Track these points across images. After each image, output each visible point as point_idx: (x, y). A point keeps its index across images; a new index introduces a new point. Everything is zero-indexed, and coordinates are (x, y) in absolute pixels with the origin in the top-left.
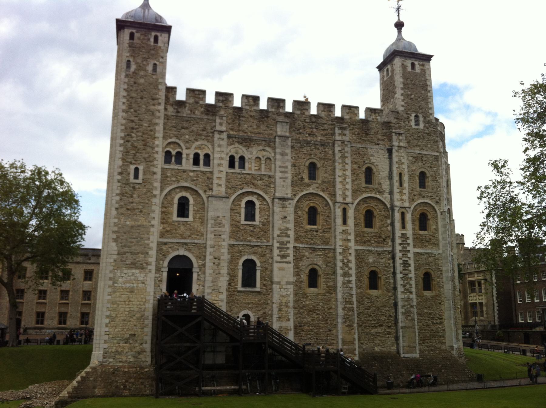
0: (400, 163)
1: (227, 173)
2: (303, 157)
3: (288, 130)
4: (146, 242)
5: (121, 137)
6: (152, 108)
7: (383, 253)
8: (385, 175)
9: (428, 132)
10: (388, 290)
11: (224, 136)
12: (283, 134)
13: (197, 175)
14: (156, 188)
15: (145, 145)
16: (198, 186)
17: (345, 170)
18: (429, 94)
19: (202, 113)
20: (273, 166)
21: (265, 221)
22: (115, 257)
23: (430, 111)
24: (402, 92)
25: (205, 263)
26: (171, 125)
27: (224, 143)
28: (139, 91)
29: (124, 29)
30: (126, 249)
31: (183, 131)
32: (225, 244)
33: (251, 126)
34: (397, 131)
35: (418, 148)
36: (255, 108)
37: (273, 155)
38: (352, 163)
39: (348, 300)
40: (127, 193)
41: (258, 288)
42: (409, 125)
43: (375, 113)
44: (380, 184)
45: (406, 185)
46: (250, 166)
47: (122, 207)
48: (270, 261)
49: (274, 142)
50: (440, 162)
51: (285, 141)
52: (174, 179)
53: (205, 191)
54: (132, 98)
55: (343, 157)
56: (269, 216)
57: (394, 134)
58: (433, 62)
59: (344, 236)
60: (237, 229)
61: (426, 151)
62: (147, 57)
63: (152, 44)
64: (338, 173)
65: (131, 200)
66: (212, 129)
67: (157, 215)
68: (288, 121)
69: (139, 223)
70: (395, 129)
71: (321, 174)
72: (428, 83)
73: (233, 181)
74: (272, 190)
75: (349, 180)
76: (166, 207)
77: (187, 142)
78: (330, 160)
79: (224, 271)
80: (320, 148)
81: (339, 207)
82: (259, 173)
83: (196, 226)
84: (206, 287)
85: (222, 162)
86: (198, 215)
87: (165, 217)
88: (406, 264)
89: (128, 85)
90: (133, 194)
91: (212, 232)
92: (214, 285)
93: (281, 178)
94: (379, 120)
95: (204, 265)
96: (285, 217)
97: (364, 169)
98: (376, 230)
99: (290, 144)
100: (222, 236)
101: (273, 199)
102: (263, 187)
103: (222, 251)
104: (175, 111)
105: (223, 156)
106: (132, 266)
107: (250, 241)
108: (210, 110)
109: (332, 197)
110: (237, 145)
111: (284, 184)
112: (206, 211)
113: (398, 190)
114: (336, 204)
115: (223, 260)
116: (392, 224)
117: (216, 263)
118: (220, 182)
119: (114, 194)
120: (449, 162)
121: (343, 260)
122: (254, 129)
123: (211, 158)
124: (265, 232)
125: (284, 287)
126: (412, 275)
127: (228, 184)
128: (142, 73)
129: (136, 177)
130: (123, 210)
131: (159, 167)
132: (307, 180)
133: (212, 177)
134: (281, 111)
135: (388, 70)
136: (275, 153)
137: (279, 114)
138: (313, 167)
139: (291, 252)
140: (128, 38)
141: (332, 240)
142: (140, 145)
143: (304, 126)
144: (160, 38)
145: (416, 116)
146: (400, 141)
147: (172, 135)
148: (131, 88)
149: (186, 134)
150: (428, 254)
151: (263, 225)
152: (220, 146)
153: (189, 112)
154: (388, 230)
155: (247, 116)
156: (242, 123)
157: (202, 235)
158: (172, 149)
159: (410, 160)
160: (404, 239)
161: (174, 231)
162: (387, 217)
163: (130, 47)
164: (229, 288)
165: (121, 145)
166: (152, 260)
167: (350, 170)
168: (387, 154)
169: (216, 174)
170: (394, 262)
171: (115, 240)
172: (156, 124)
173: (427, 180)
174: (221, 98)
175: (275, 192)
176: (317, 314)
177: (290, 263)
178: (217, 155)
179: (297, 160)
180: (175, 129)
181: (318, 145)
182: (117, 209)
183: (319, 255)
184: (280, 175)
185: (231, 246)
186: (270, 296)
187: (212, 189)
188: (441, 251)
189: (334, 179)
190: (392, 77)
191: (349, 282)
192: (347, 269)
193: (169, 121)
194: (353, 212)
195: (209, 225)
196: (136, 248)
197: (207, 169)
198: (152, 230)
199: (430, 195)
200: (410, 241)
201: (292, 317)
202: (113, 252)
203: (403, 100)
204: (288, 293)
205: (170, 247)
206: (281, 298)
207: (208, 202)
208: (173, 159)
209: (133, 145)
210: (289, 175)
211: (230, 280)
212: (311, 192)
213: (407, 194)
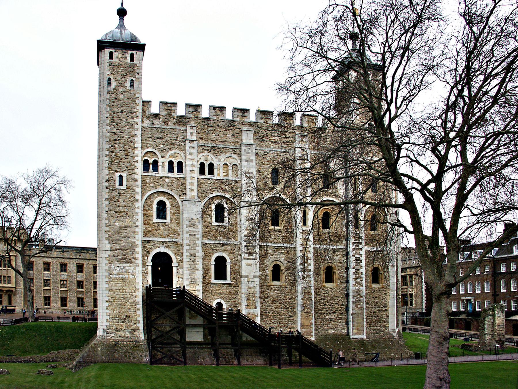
3: (252, 138)
4: (132, 240)
10: (342, 283)
14: (138, 193)
16: (173, 191)
19: (174, 124)
22: (109, 253)
25: (182, 259)
26: (147, 136)
27: (194, 151)
28: (120, 105)
30: (117, 247)
31: (158, 141)
32: (199, 242)
37: (239, 161)
39: (306, 291)
40: (114, 198)
41: (228, 281)
46: (218, 172)
48: (239, 257)
52: (152, 185)
53: (180, 196)
54: (114, 112)
63: (129, 61)
67: (140, 217)
69: (126, 224)
76: (147, 210)
79: (200, 266)
83: (173, 227)
84: (185, 280)
85: (194, 169)
86: (174, 217)
88: (358, 261)
91: (187, 232)
92: (191, 278)
95: (182, 261)
100: (196, 236)
103: (197, 248)
104: (151, 123)
105: (195, 163)
107: (220, 240)
108: (182, 120)
110: (206, 153)
115: (198, 256)
123: (184, 165)
124: (234, 232)
125: (251, 280)
126: (363, 270)
128: (121, 89)
129: (121, 184)
130: (112, 213)
136: (241, 160)
137: (243, 123)
139: (257, 250)
140: (108, 58)
144: (135, 56)
148: (113, 104)
152: (191, 154)
153: (163, 124)
155: (215, 125)
156: (210, 132)
157: (179, 235)
164: (204, 281)
166: (139, 256)
169: (188, 181)
171: (108, 239)
174: (191, 109)
176: (280, 303)
178: (189, 163)
185: (205, 244)
186: (239, 288)
187: (185, 194)
191: (308, 276)
195: (185, 226)
196: (124, 246)
198: (137, 230)
201: (258, 305)
202: (107, 249)
204: (255, 285)
206: (249, 290)
208: (151, 166)
209: (116, 155)
211: (204, 273)
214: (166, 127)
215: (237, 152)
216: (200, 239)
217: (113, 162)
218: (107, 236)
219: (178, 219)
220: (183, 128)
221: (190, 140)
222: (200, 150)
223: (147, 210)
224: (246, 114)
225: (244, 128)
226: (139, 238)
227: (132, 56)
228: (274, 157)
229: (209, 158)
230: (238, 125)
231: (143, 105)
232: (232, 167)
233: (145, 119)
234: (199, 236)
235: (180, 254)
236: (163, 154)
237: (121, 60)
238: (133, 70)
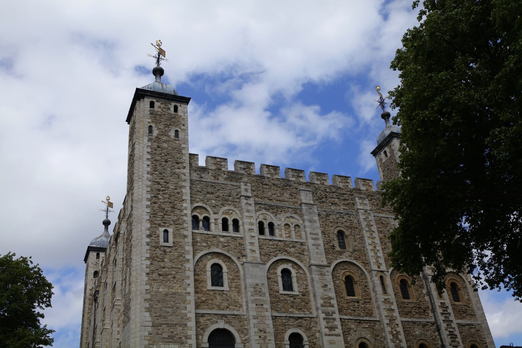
1: (259, 239)
2: (330, 225)
3: (312, 199)
4: (182, 312)
5: (147, 199)
7: (427, 325)
11: (251, 201)
12: (308, 202)
13: (227, 240)
14: (188, 251)
16: (230, 252)
17: (374, 238)
21: (304, 290)
22: (150, 329)
27: (252, 208)
32: (268, 314)
33: (275, 194)
36: (276, 177)
37: (301, 222)
40: (157, 257)
47: (153, 272)
49: (301, 210)
52: (205, 244)
54: (156, 160)
55: (369, 226)
59: (388, 306)
60: (277, 299)
62: (169, 124)
63: (173, 112)
64: (368, 241)
65: (162, 264)
66: (237, 195)
69: (173, 291)
71: (350, 243)
73: (265, 248)
74: (306, 258)
75: (379, 248)
76: (198, 275)
77: (213, 207)
78: (357, 228)
80: (344, 217)
81: (376, 276)
83: (233, 296)
85: (253, 227)
86: (234, 284)
91: (253, 302)
93: (314, 245)
98: (415, 301)
99: (316, 211)
100: (265, 306)
103: (267, 322)
104: (199, 176)
105: (253, 221)
106: (170, 340)
107: (292, 313)
110: (264, 211)
115: (269, 333)
116: (429, 294)
117: (262, 337)
118: (254, 248)
119: (144, 258)
121: (392, 332)
122: (278, 196)
123: (240, 223)
124: (307, 303)
128: (164, 138)
129: (166, 240)
130: (155, 276)
132: (338, 248)
134: (301, 180)
135: (385, 153)
136: (304, 220)
138: (340, 234)
139: (338, 323)
140: (149, 106)
141: (376, 312)
142: (168, 207)
144: (179, 108)
147: (198, 199)
148: (155, 152)
149: (212, 199)
150: (469, 325)
151: (303, 295)
152: (248, 211)
153: (213, 178)
154: (425, 301)
155: (270, 184)
156: (265, 190)
157: (241, 306)
158: (199, 213)
160: (444, 309)
161: (210, 301)
165: (147, 207)
166: (192, 333)
169: (248, 240)
170: (440, 334)
171: (148, 310)
172: (184, 187)
174: (242, 166)
175: (310, 260)
177: (340, 335)
178: (246, 220)
179: (325, 228)
180: (200, 194)
181: (342, 213)
182: (147, 274)
183: (366, 328)
185: (274, 318)
188: (479, 322)
192: (397, 342)
195: (249, 294)
198: (188, 298)
200: (450, 310)
202: (147, 324)
205: (208, 320)
208: (201, 223)
209: (159, 207)
210: (321, 242)
212: (345, 260)
214: (216, 181)
216: (269, 310)
217: (156, 214)
218: (148, 306)
219: (238, 287)
221: (245, 196)
223: (198, 275)
224: (301, 175)
226: (191, 311)
227: (176, 109)
228: (337, 219)
229: (268, 217)
230: (294, 185)
231: (190, 158)
233: (192, 171)
234: (267, 306)
235: (244, 331)
237: (164, 110)
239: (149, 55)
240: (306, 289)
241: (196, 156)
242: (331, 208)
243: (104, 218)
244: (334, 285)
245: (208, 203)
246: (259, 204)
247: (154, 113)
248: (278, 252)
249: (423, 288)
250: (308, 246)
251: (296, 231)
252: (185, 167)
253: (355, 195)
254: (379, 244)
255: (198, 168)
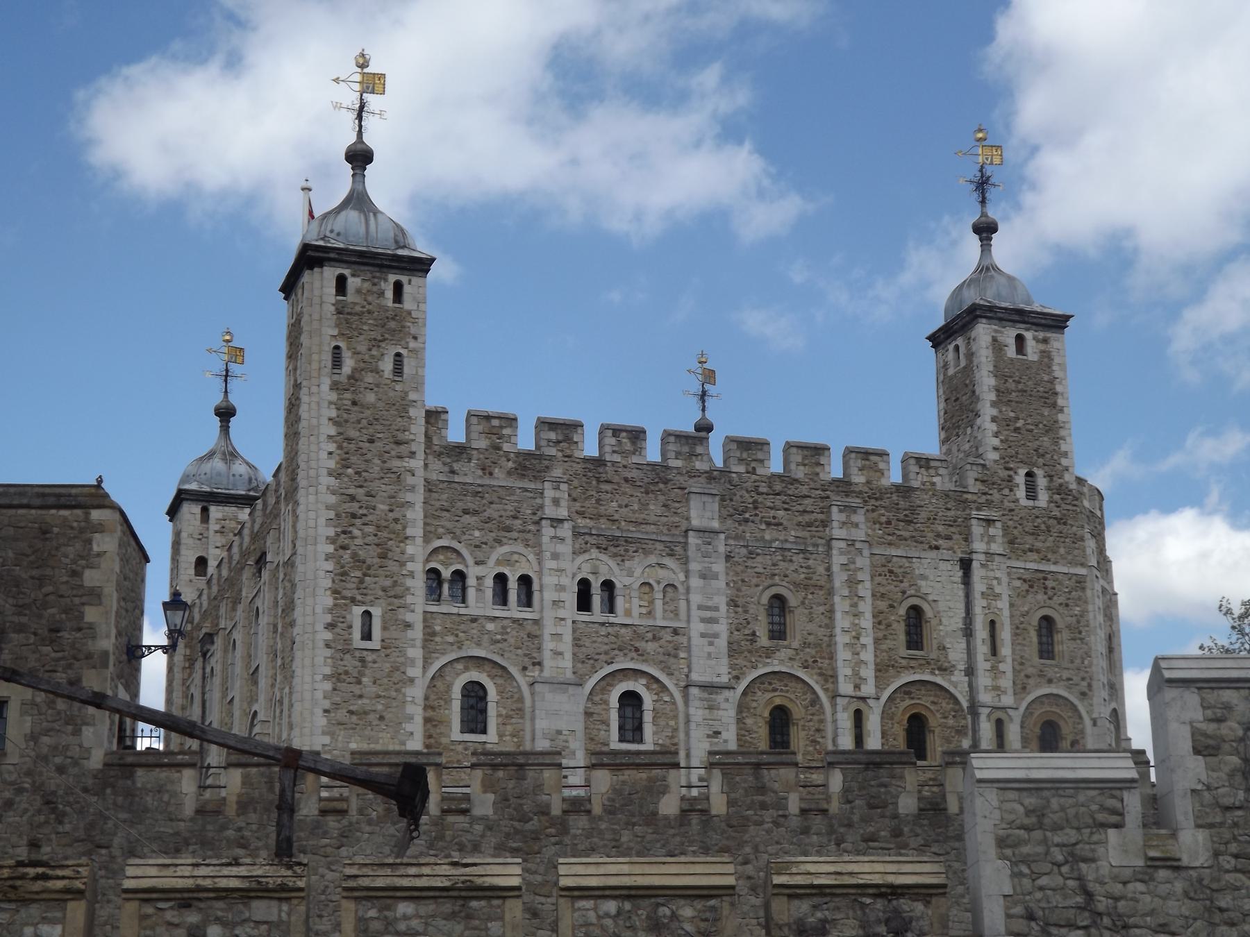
0: (990, 595)
3: (716, 516)
5: (327, 538)
6: (396, 463)
8: (954, 627)
9: (1058, 514)
11: (566, 531)
13: (504, 628)
15: (383, 556)
18: (1061, 417)
20: (683, 604)
23: (1064, 462)
24: (994, 412)
26: (438, 504)
27: (566, 549)
28: (364, 422)
29: (321, 266)
31: (467, 519)
34: (984, 514)
35: (1034, 556)
36: (635, 459)
37: (682, 577)
38: (873, 595)
40: (346, 673)
42: (1011, 498)
43: (928, 468)
44: (944, 648)
45: (1006, 651)
46: (627, 605)
49: (685, 545)
50: (1089, 593)
51: (709, 544)
52: (451, 639)
53: (525, 669)
54: (349, 440)
55: (853, 583)
56: (675, 730)
57: (974, 522)
58: (1068, 343)
61: (1055, 563)
62: (380, 338)
63: (390, 304)
64: (842, 622)
65: (357, 690)
66: (534, 514)
68: (714, 492)
70: (978, 509)
71: (799, 624)
72: (1059, 388)
75: (867, 640)
76: (433, 708)
77: (476, 546)
81: (845, 709)
82: (651, 623)
85: (564, 596)
86: (509, 727)
87: (432, 731)
89: (338, 409)
90: (362, 674)
93: (703, 635)
94: (939, 487)
96: (717, 733)
97: (902, 611)
101: (687, 687)
102: (661, 658)
104: (447, 469)
105: (565, 581)
108: (529, 465)
109: (826, 681)
110: (594, 553)
111: (711, 649)
112: (528, 716)
113: (988, 665)
114: (839, 700)
118: (561, 647)
120: (1117, 587)
122: (634, 512)
123: (535, 586)
127: (577, 649)
128: (369, 378)
129: (367, 636)
130: (341, 714)
131: (419, 609)
132: (764, 641)
133: (538, 633)
134: (699, 465)
135: (957, 348)
136: (687, 574)
138: (779, 603)
142: (370, 555)
143: (755, 502)
144: (407, 289)
145: (1029, 474)
146: (991, 539)
147: (441, 530)
148: (345, 416)
152: (555, 556)
153: (480, 472)
155: (616, 479)
158: (443, 563)
159: (1015, 588)
162: (961, 732)
163: (339, 312)
165: (328, 557)
167: (868, 615)
168: (960, 574)
169: (549, 628)
172: (409, 504)
173: (1057, 637)
175: (690, 671)
178: (550, 580)
179: (739, 590)
182: (326, 711)
184: (702, 627)
187: (539, 664)
189: (832, 636)
190: (969, 370)
193: (434, 495)
194: (879, 719)
197: (527, 614)
199: (1065, 675)
203: (996, 435)
207: (532, 694)
208: (446, 586)
209: (354, 556)
210: (722, 628)
212: (776, 669)
213: (1010, 675)
214: (487, 481)
215: (676, 549)
220: (532, 486)
221: (551, 519)
222: (577, 546)
223: (433, 708)
224: (699, 450)
225: (695, 485)
227: (398, 287)
230: (678, 477)
231: (427, 422)
232: (664, 592)
233: (430, 457)
236: (480, 555)
237: (370, 298)
238: (397, 326)
239: (338, 106)
240: (672, 737)
241: (443, 416)
242: (763, 538)
243: (218, 399)
244: (739, 729)
245: (466, 537)
246: (585, 534)
247: (346, 310)
248: (616, 652)
249: (966, 734)
250: (689, 639)
251: (667, 599)
252: (414, 453)
253: (833, 497)
254: (870, 631)
255: (445, 447)
